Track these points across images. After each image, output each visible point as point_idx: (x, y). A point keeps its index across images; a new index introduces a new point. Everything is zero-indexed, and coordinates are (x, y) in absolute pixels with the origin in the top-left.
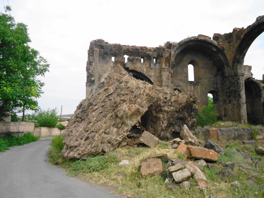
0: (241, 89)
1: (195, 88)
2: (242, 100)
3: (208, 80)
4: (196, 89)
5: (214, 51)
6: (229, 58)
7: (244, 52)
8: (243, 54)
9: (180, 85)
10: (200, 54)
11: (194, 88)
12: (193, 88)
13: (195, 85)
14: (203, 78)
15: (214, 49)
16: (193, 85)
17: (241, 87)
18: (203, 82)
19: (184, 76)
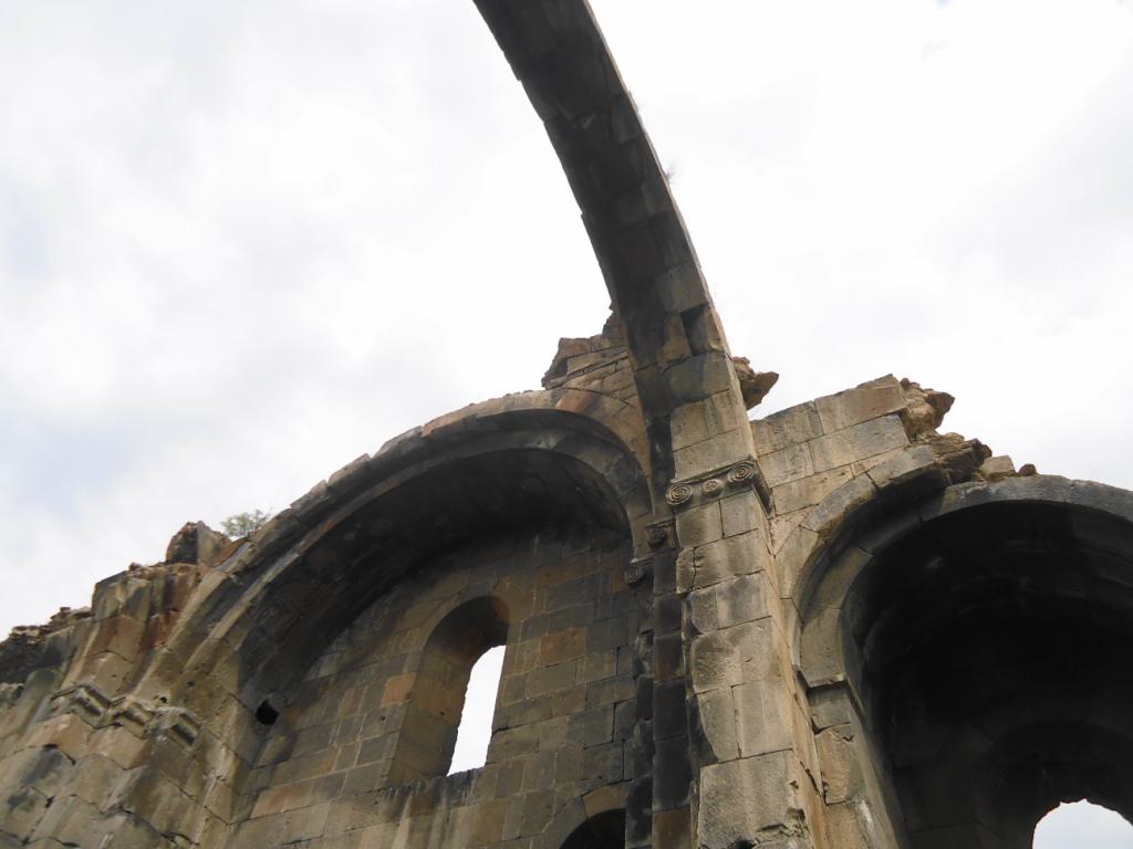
0: (705, 634)
1: (429, 829)
2: (727, 792)
3: (578, 710)
4: (435, 835)
5: (548, 453)
6: (625, 434)
7: (680, 302)
8: (675, 320)
9: (299, 841)
10: (537, 540)
11: (418, 836)
12: (412, 830)
13: (434, 802)
14: (526, 706)
15: (542, 445)
16: (412, 814)
17: (711, 616)
18: (524, 746)
19: (365, 744)
